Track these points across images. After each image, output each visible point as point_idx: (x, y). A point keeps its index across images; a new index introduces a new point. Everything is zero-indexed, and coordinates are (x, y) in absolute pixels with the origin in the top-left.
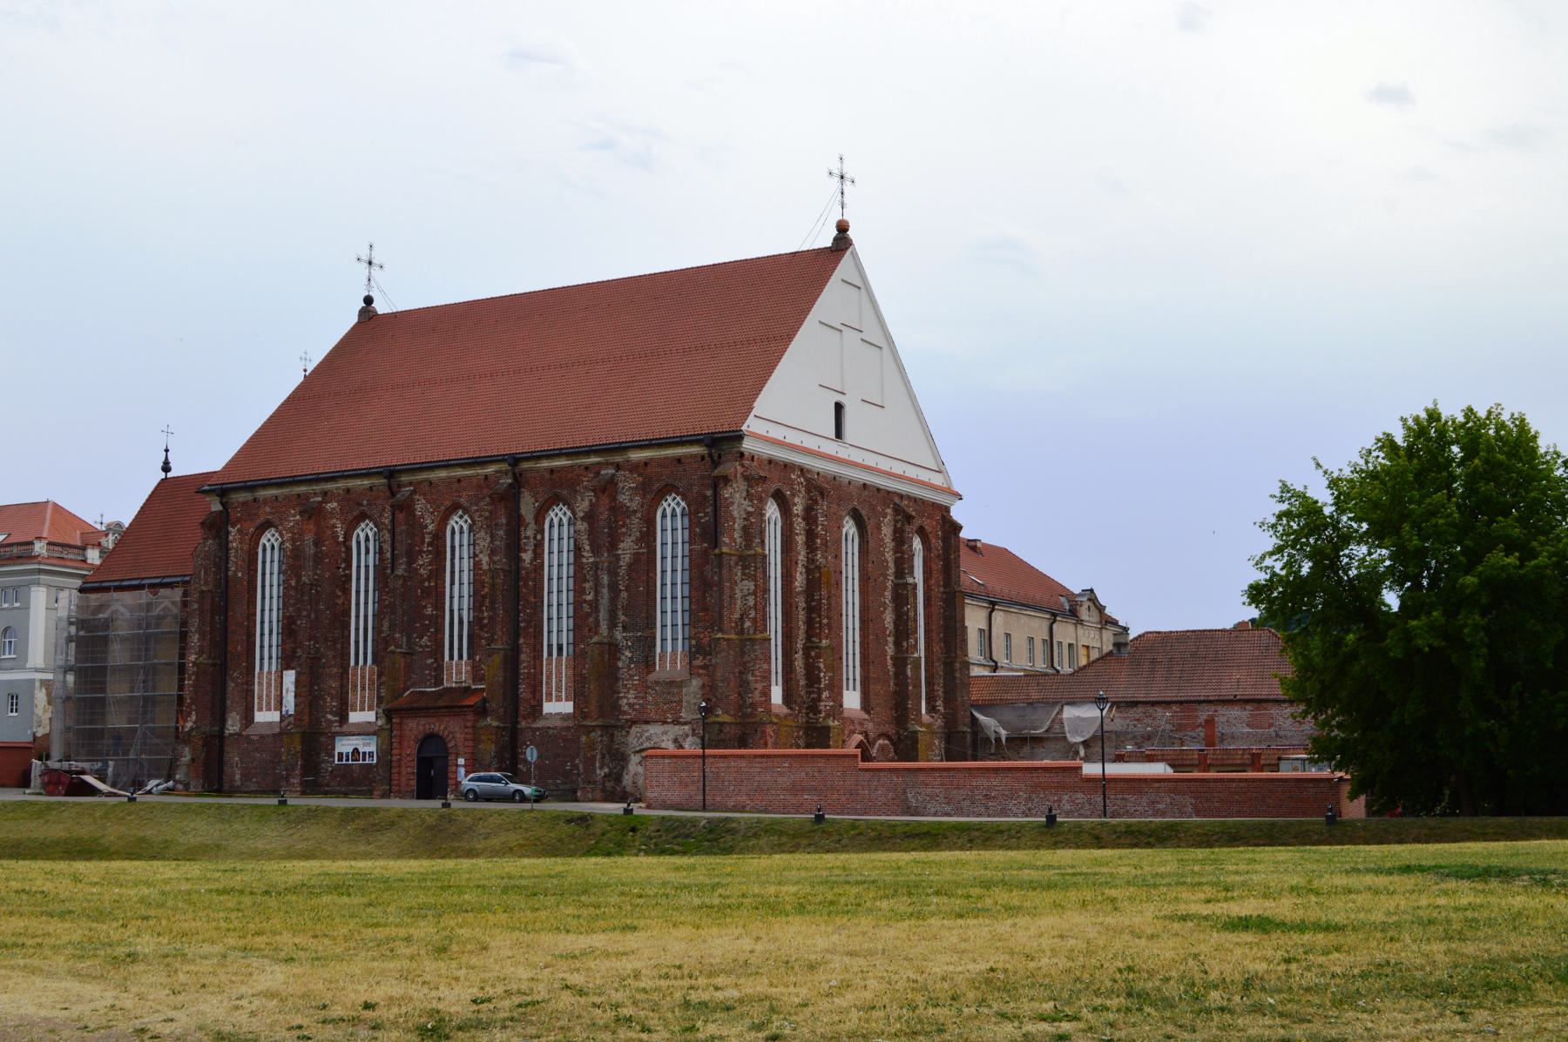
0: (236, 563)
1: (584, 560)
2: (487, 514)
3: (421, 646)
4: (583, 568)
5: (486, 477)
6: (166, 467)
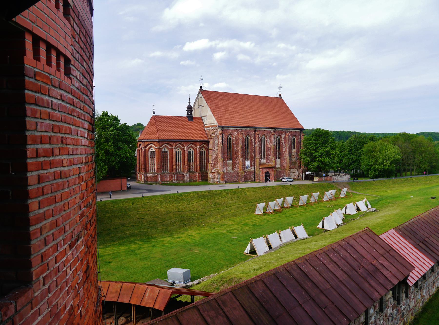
6: (154, 113)
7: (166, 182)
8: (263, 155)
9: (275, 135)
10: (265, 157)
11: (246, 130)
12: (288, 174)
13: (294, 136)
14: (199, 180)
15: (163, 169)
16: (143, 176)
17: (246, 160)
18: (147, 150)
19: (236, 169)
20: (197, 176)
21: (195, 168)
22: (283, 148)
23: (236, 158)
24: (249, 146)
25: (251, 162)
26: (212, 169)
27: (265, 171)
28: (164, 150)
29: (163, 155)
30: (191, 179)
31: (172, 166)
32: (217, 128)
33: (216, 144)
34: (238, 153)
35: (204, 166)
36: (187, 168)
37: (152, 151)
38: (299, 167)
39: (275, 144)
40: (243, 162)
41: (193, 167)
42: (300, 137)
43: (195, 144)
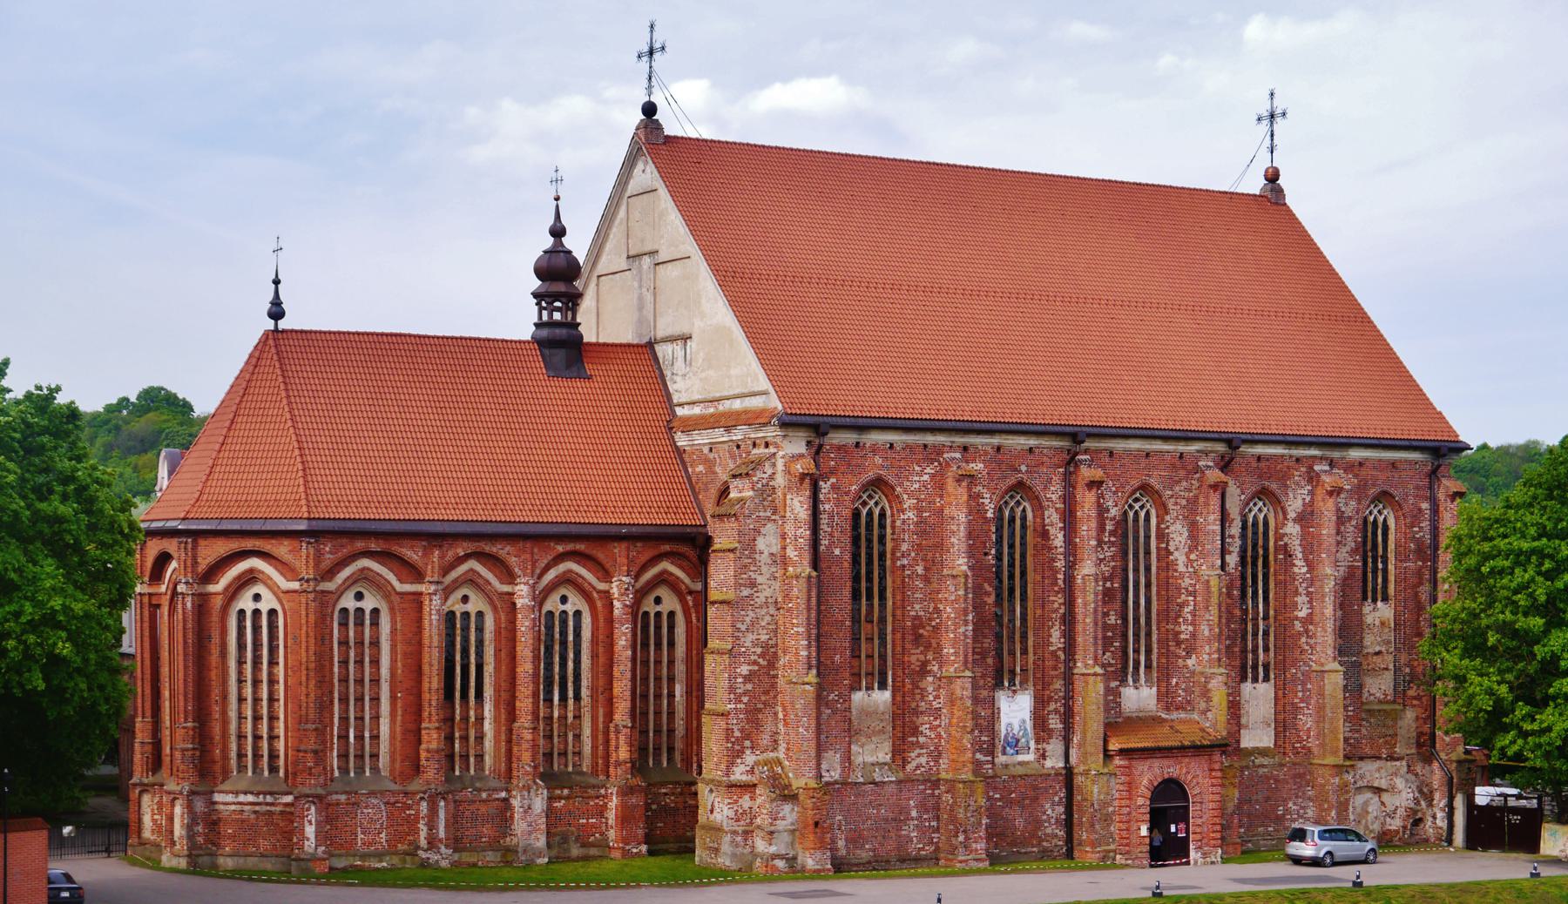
0: (831, 535)
1: (1296, 570)
4: (1294, 579)
6: (277, 312)
7: (364, 857)
8: (1137, 651)
9: (1233, 491)
10: (1148, 667)
11: (999, 449)
12: (1333, 798)
13: (1384, 497)
14: (626, 841)
15: (344, 756)
16: (178, 810)
17: (998, 684)
18: (218, 602)
19: (923, 760)
20: (611, 816)
21: (594, 747)
22: (1297, 593)
23: (923, 671)
24: (1023, 574)
25: (1040, 703)
26: (735, 755)
27: (1148, 774)
28: (348, 602)
29: (344, 643)
30: (565, 840)
31: (412, 735)
32: (772, 433)
33: (765, 558)
34: (936, 629)
35: (671, 731)
36: (535, 746)
37: (257, 612)
38: (1426, 747)
39: (1233, 560)
40: (976, 700)
41: (578, 737)
42: (1425, 506)
43: (600, 556)
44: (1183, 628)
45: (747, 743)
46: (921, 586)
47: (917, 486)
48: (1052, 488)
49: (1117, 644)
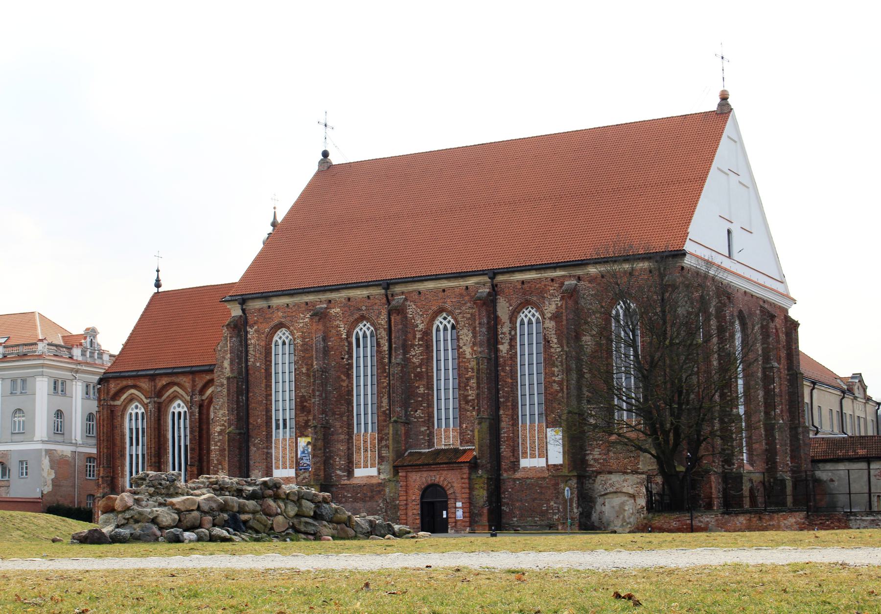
1: (553, 350)
2: (469, 316)
3: (415, 417)
5: (467, 288)
6: (158, 284)
27: (418, 480)
44: (470, 392)
45: (220, 467)
46: (305, 379)
47: (301, 325)
48: (382, 317)
49: (425, 405)
